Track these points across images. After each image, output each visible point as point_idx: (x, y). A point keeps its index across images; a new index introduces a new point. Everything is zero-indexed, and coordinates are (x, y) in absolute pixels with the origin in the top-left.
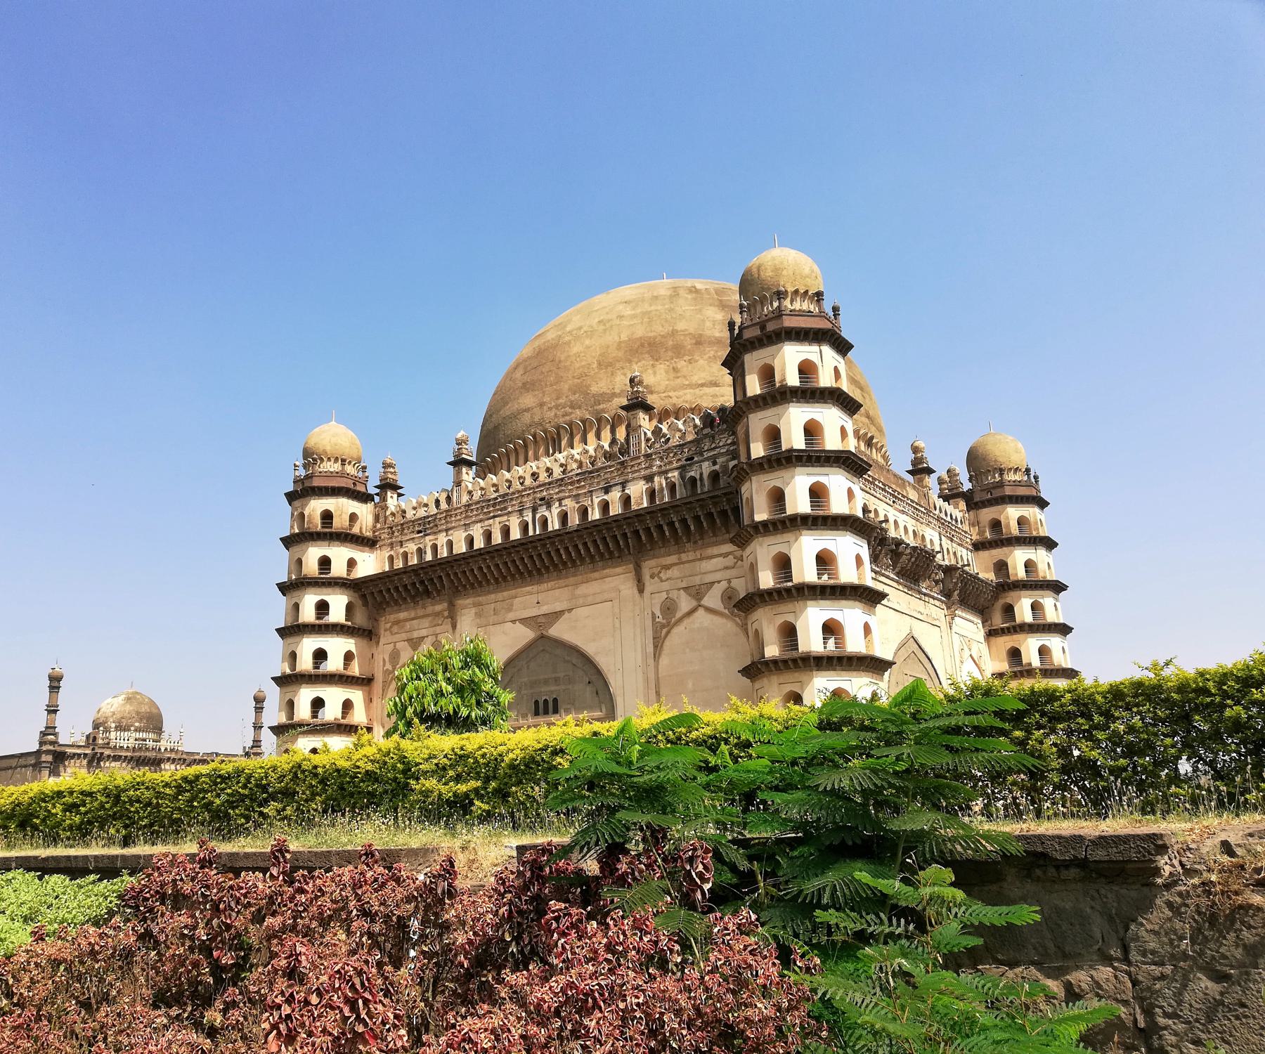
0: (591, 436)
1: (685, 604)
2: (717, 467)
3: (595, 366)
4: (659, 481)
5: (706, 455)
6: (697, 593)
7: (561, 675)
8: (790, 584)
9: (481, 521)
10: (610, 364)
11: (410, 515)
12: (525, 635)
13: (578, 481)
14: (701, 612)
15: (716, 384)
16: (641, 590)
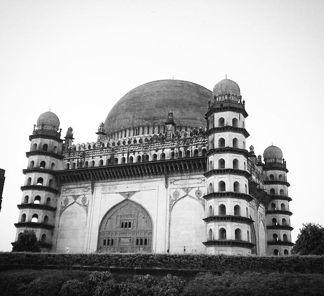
0: (151, 131)
1: (182, 193)
2: (197, 148)
4: (176, 150)
6: (187, 190)
8: (224, 192)
10: (161, 107)
11: (77, 150)
12: (122, 198)
13: (146, 146)
15: (195, 120)
16: (167, 187)
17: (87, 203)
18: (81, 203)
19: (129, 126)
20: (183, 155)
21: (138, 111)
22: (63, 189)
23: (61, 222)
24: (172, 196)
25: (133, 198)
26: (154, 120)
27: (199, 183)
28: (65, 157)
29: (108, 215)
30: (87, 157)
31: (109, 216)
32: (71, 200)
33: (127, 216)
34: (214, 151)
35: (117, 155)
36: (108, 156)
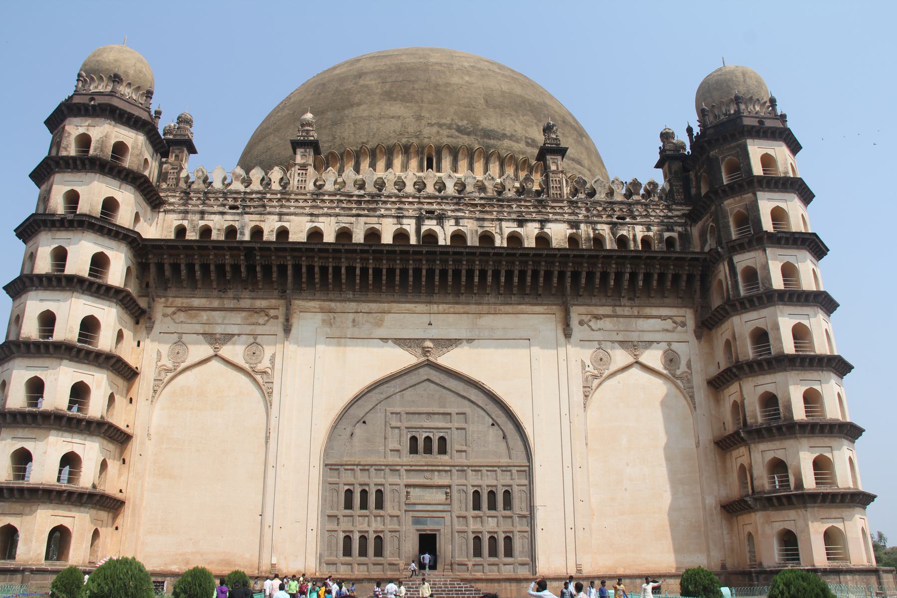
2: (651, 234)
3: (482, 101)
5: (639, 220)
7: (453, 410)
8: (812, 353)
9: (337, 215)
10: (499, 107)
11: (218, 185)
12: (405, 358)
13: (483, 205)
15: (580, 163)
16: (568, 334)
17: (265, 364)
19: (404, 140)
20: (610, 244)
21: (430, 103)
22: (160, 308)
23: (155, 421)
24: (588, 362)
25: (449, 359)
26: (489, 138)
27: (664, 329)
29: (351, 411)
30: (261, 214)
31: (358, 412)
33: (429, 414)
34: (758, 239)
35: (375, 220)
36: (340, 218)
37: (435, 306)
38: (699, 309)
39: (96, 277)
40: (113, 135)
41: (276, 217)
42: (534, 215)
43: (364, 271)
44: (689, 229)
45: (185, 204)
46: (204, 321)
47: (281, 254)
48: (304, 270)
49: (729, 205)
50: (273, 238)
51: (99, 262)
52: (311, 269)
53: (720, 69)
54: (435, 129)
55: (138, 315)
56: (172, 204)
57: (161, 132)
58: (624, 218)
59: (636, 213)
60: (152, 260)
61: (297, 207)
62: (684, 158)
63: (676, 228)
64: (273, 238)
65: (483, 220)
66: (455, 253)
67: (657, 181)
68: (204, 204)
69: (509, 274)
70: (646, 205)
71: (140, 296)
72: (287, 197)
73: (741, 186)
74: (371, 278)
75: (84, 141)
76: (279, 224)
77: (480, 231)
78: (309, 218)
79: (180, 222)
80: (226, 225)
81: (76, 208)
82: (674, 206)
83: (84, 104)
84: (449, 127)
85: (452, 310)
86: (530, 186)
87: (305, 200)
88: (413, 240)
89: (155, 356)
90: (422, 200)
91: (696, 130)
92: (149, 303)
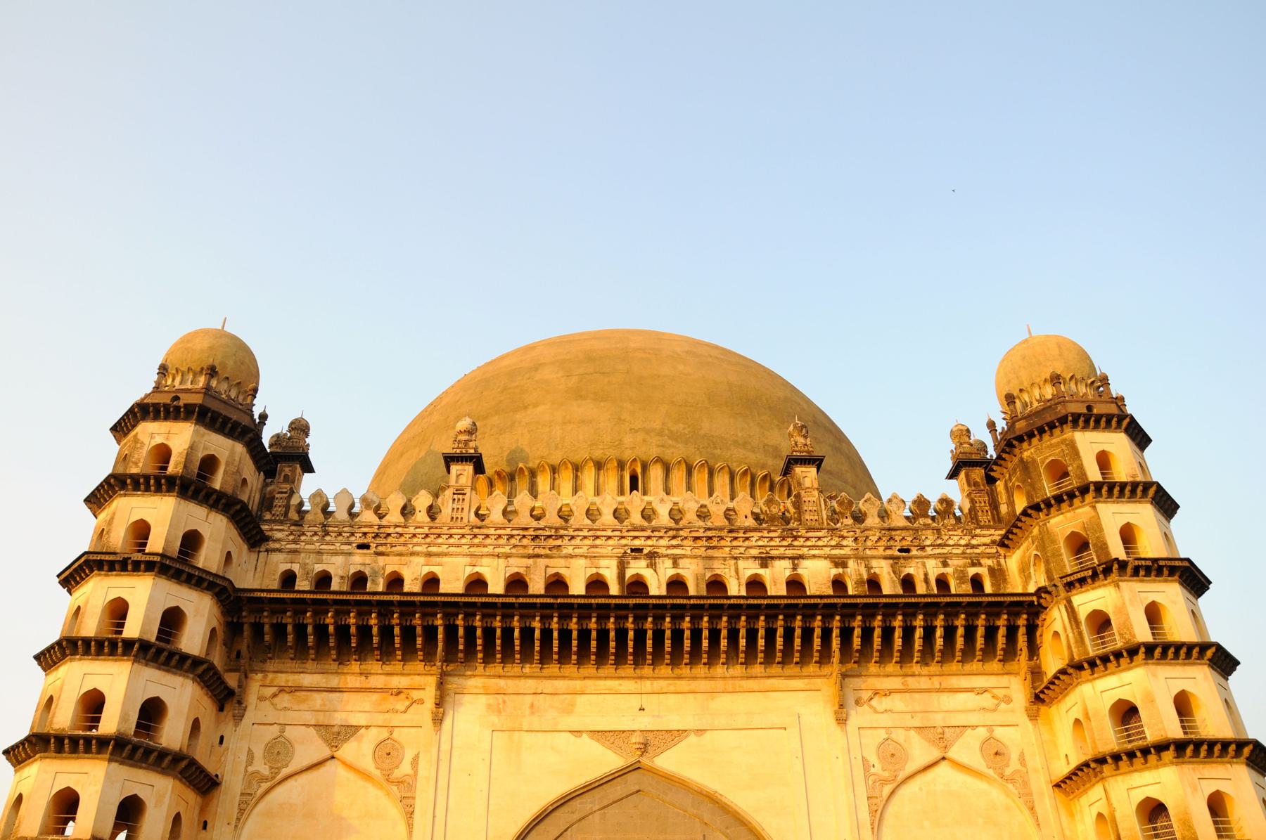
2: (949, 570)
6: (942, 737)
9: (507, 556)
13: (710, 538)
14: (943, 768)
16: (842, 721)
17: (405, 768)
18: (368, 764)
19: (598, 454)
22: (256, 688)
24: (873, 759)
25: (667, 761)
28: (267, 539)
30: (401, 555)
32: (309, 748)
35: (562, 562)
37: (648, 683)
38: (1029, 677)
39: (168, 642)
40: (201, 446)
41: (422, 560)
42: (782, 549)
43: (547, 633)
44: (1002, 561)
45: (294, 542)
46: (318, 707)
47: (429, 610)
48: (461, 632)
49: (1057, 524)
50: (417, 588)
51: (172, 620)
52: (470, 631)
53: (1026, 341)
54: (640, 437)
55: (225, 697)
56: (279, 540)
57: (266, 441)
58: (908, 551)
59: (928, 542)
60: (247, 618)
61: (451, 545)
62: (986, 464)
63: (983, 561)
64: (417, 588)
65: (710, 558)
66: (674, 606)
67: (951, 496)
68: (322, 540)
69: (752, 635)
70: (938, 530)
71: (227, 671)
72: (438, 531)
73: (1071, 496)
74: (555, 643)
75: (163, 453)
76: (426, 569)
77: (708, 575)
78: (467, 560)
79: (288, 566)
80: (352, 571)
81: (145, 545)
82: (978, 531)
83: (165, 405)
84: (660, 433)
85: (672, 689)
86: (775, 510)
87: (463, 536)
88: (614, 589)
89: (244, 757)
90: (626, 534)
91: (1001, 425)
92: (240, 681)
